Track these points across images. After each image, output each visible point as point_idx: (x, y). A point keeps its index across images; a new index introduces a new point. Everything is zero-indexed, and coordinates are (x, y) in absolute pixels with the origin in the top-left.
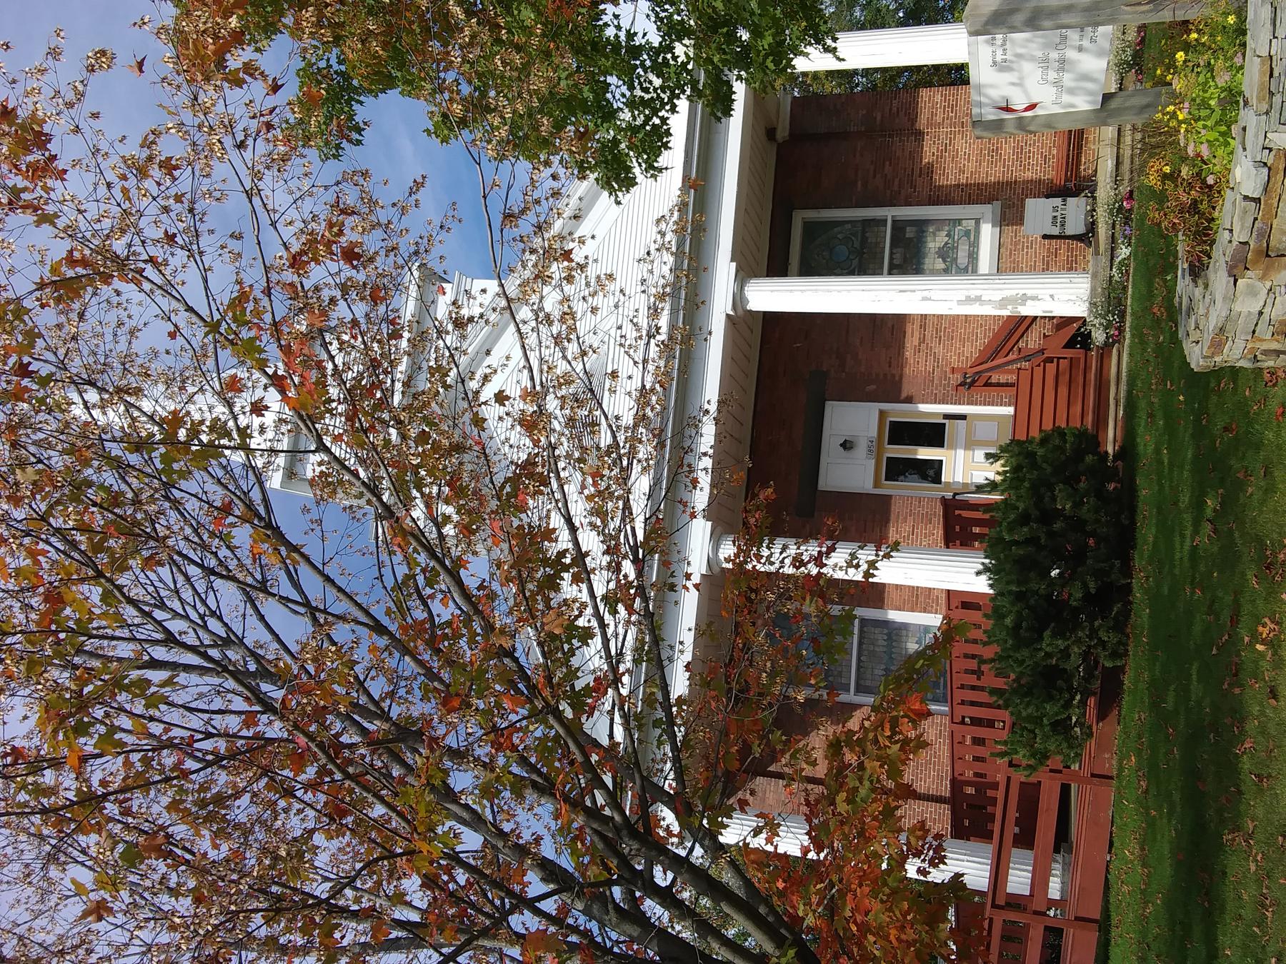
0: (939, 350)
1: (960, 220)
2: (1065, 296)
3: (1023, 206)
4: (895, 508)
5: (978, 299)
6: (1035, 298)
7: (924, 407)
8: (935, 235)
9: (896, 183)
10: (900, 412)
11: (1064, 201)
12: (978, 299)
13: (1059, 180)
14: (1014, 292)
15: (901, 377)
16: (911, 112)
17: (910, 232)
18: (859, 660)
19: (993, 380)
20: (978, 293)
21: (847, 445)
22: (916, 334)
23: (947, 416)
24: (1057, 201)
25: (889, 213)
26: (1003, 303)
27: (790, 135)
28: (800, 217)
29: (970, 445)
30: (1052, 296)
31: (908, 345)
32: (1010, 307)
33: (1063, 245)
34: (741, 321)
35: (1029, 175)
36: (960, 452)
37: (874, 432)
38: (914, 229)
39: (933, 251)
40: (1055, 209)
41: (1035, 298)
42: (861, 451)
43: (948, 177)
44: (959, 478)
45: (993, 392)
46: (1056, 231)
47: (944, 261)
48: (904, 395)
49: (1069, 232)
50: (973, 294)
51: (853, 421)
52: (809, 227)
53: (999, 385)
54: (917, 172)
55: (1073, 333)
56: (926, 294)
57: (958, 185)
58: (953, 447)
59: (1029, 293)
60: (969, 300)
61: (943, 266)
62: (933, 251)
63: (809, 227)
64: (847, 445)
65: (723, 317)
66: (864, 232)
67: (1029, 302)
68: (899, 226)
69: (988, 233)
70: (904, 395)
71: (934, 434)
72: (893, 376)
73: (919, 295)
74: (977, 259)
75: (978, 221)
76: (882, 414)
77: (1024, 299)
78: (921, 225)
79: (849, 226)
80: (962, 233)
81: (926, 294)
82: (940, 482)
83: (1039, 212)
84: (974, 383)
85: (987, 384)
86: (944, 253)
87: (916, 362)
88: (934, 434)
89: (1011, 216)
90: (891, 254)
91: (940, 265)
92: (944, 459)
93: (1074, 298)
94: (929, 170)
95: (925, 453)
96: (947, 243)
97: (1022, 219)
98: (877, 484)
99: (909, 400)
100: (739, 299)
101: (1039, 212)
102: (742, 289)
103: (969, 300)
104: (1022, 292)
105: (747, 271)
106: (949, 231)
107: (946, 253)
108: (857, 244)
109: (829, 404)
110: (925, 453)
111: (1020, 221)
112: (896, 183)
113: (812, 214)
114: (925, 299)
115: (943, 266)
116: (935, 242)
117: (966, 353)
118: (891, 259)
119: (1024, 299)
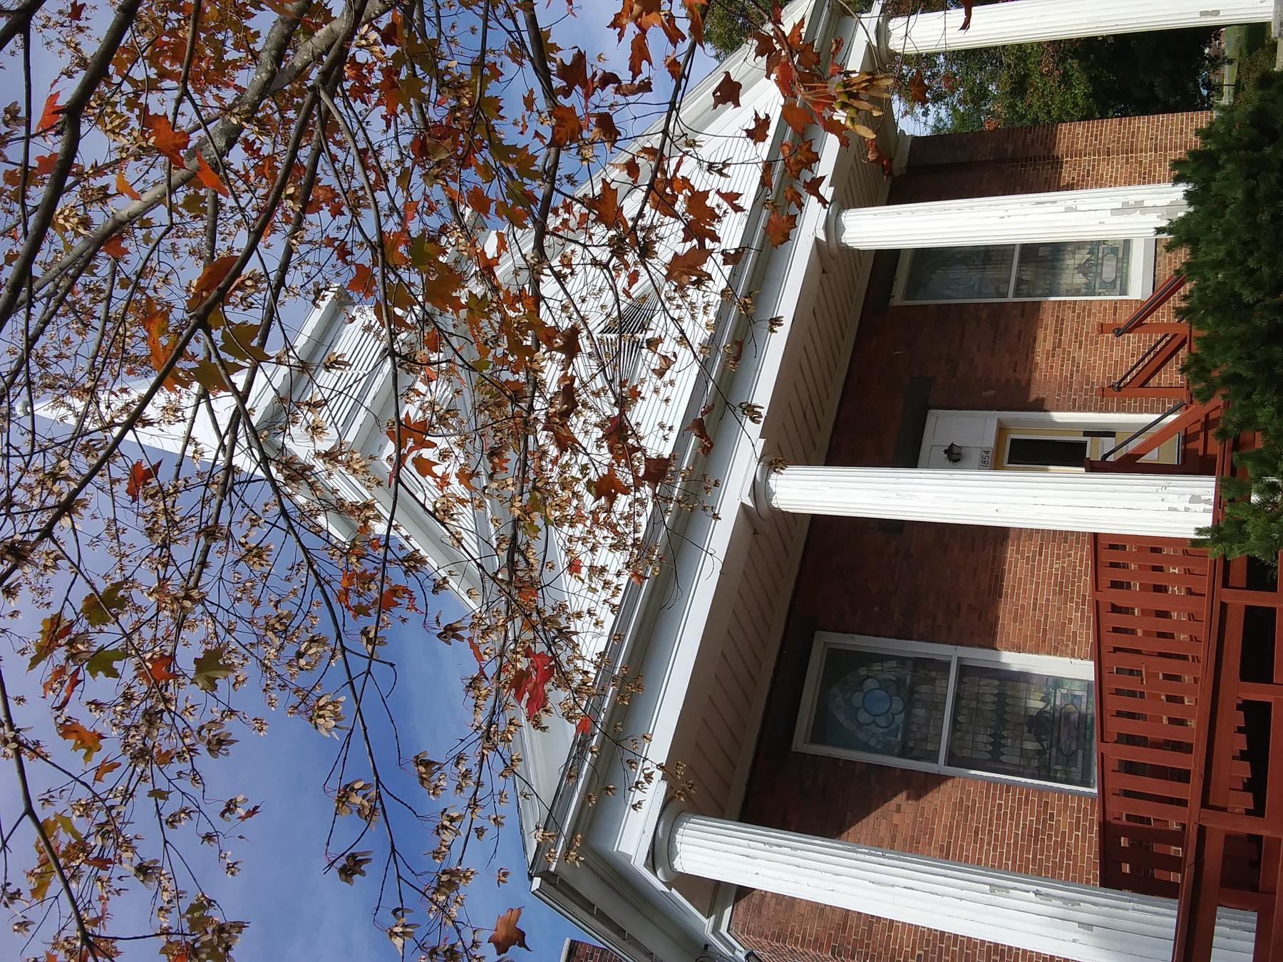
0: (1080, 355)
7: (1059, 417)
10: (1026, 425)
15: (1029, 382)
16: (1049, 141)
18: (954, 721)
22: (1050, 339)
27: (908, 167)
31: (1039, 350)
48: (1033, 397)
56: (1070, 203)
70: (1033, 397)
76: (1002, 430)
86: (1083, 269)
99: (1039, 406)
102: (838, 215)
114: (1069, 210)
115: (1084, 280)
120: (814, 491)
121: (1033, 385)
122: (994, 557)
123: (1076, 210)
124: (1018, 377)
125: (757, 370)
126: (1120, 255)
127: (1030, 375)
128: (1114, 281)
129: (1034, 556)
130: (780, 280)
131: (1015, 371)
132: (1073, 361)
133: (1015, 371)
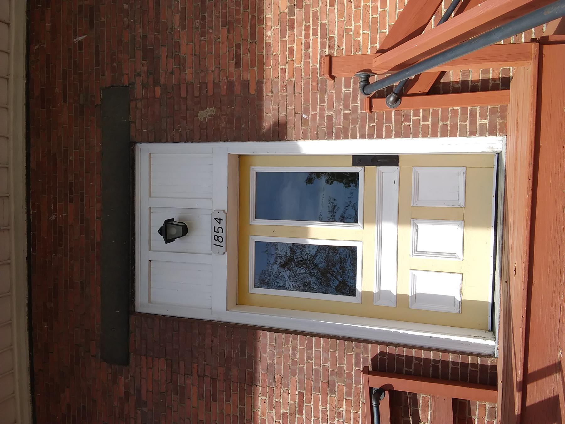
4: (264, 358)
7: (308, 147)
10: (266, 155)
15: (260, 84)
19: (454, 75)
23: (359, 160)
29: (411, 213)
31: (268, 14)
36: (389, 227)
42: (202, 237)
45: (452, 104)
48: (268, 123)
53: (465, 87)
58: (376, 219)
70: (268, 123)
71: (339, 192)
72: (245, 85)
76: (241, 163)
82: (352, 292)
85: (439, 88)
88: (339, 192)
92: (359, 245)
98: (240, 298)
99: (278, 133)
109: (144, 152)
110: (324, 234)
121: (267, 92)
122: (242, 411)
124: (245, 76)
127: (261, 71)
129: (292, 414)
132: (323, 36)
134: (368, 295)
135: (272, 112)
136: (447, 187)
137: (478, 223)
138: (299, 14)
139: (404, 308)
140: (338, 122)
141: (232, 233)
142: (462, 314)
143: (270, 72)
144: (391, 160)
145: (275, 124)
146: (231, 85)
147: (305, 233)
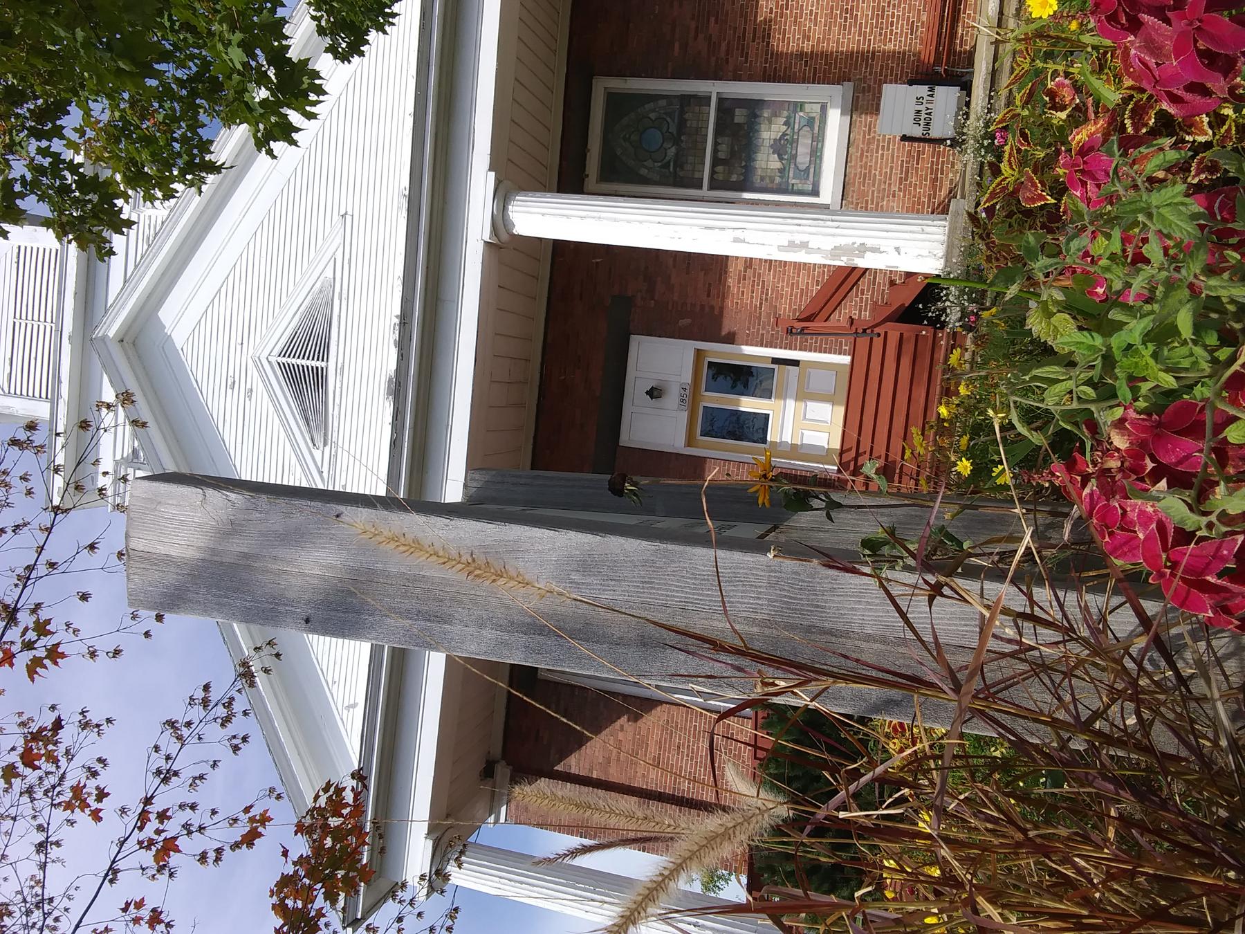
1: (802, 104)
2: (915, 248)
3: (880, 92)
5: (804, 245)
6: (875, 250)
7: (748, 350)
8: (770, 122)
9: (724, 45)
10: (720, 352)
11: (932, 90)
12: (804, 245)
13: (928, 57)
14: (849, 241)
15: (722, 309)
17: (740, 116)
20: (805, 238)
21: (654, 393)
23: (776, 361)
24: (923, 90)
25: (714, 88)
26: (837, 251)
28: (602, 86)
29: (804, 395)
30: (897, 249)
32: (844, 259)
33: (928, 148)
34: (506, 248)
35: (890, 47)
36: (791, 403)
37: (687, 378)
38: (744, 111)
39: (767, 143)
40: (919, 100)
41: (875, 250)
42: (672, 400)
43: (792, 39)
44: (787, 438)
46: (918, 131)
47: (781, 159)
49: (935, 133)
50: (798, 239)
51: (662, 361)
52: (616, 102)
54: (749, 35)
55: (919, 302)
56: (739, 234)
57: (802, 53)
58: (783, 396)
59: (870, 243)
60: (792, 245)
61: (778, 165)
62: (767, 143)
63: (616, 102)
64: (654, 393)
65: (480, 246)
66: (682, 112)
67: (868, 254)
68: (726, 106)
69: (836, 121)
72: (712, 308)
73: (730, 234)
74: (821, 158)
75: (824, 109)
76: (699, 353)
77: (863, 249)
78: (754, 106)
79: (663, 103)
80: (803, 122)
81: (739, 234)
82: (764, 441)
83: (900, 102)
84: (807, 325)
87: (739, 298)
89: (864, 103)
90: (716, 144)
91: (775, 163)
92: (771, 413)
93: (925, 253)
94: (764, 32)
95: (748, 404)
96: (784, 134)
97: (878, 109)
98: (690, 441)
99: (730, 339)
100: (500, 222)
101: (900, 102)
102: (504, 209)
103: (792, 245)
104: (859, 241)
105: (514, 178)
106: (788, 118)
107: (783, 147)
108: (673, 129)
109: (635, 340)
110: (748, 404)
111: (875, 109)
112: (724, 45)
113: (616, 84)
114: (736, 240)
115: (778, 165)
116: (770, 132)
117: (789, 305)
118: (715, 151)
119: (863, 249)
120: (550, 219)
121: (725, 312)
123: (744, 241)
124: (713, 303)
125: (448, 426)
126: (816, 129)
128: (808, 168)
130: (456, 302)
131: (709, 295)
132: (763, 287)
133: (709, 295)
134: (774, 444)
135: (727, 326)
136: (828, 382)
137: (839, 404)
138: (750, 272)
139: (795, 451)
140: (767, 338)
141: (692, 397)
142: (824, 455)
143: (729, 303)
144: (795, 363)
145: (729, 333)
146: (702, 306)
147: (738, 403)
